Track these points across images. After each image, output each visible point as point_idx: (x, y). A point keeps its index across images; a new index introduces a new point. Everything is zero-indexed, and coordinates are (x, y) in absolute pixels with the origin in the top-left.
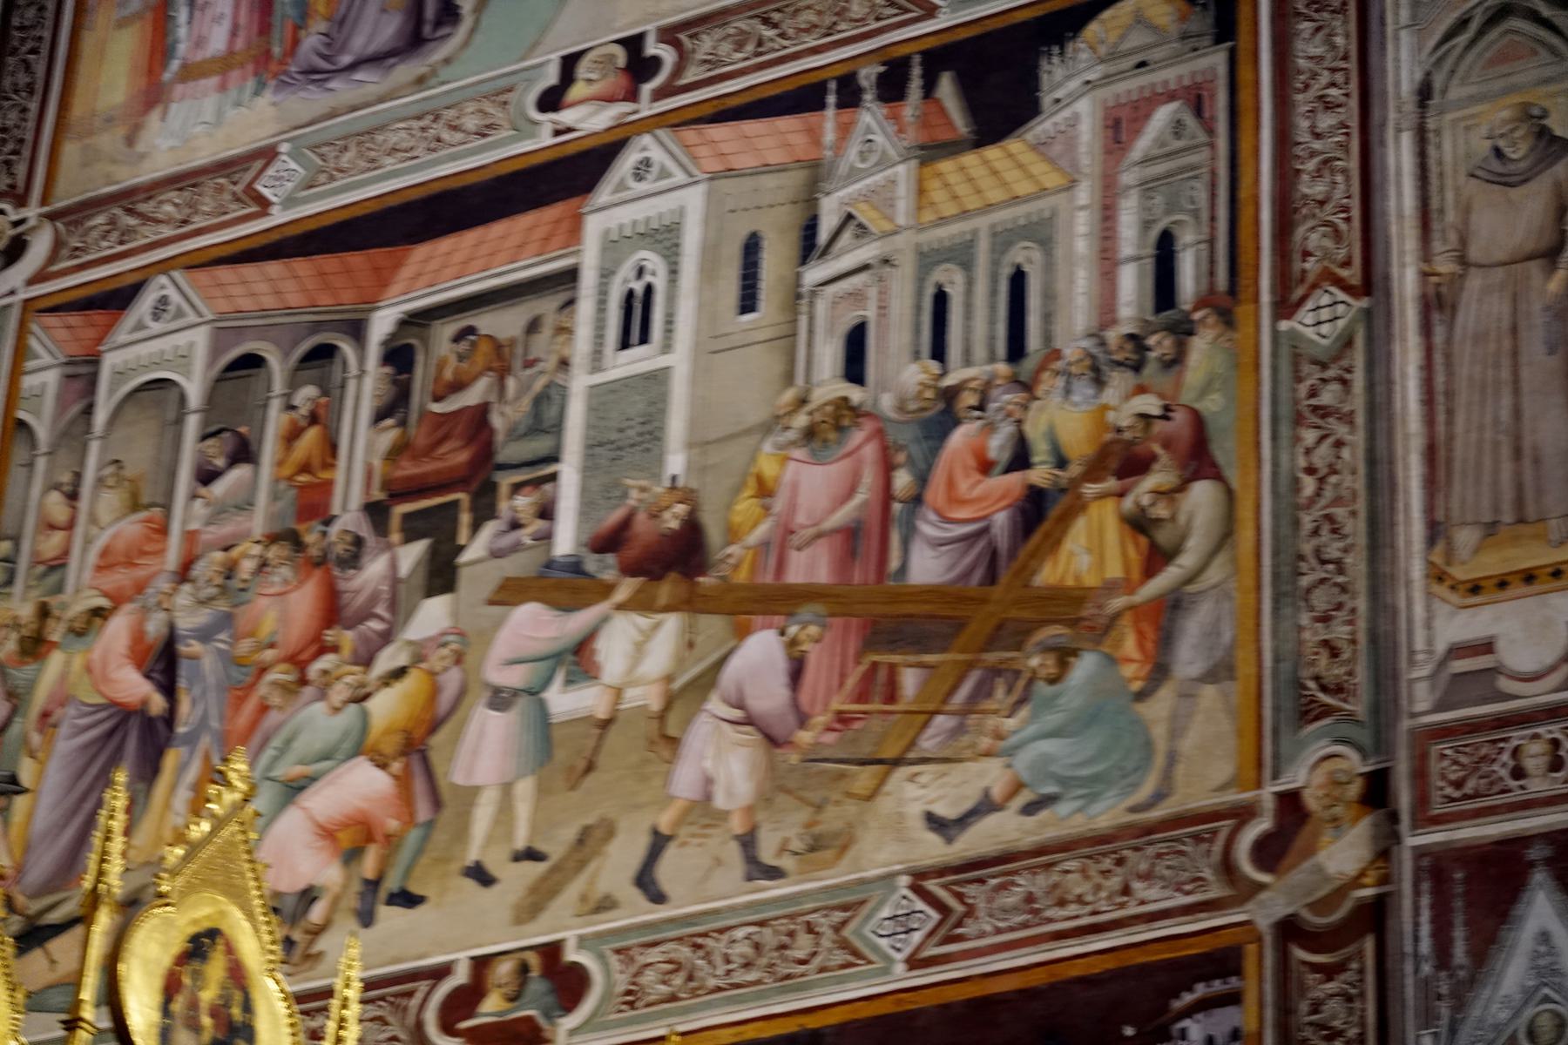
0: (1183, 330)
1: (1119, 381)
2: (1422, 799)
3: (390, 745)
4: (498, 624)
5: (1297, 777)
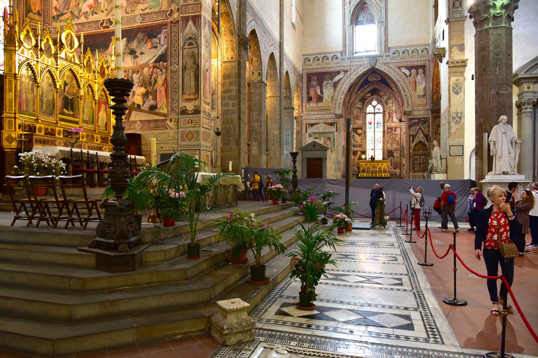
2: (181, 12)
5: (172, 8)
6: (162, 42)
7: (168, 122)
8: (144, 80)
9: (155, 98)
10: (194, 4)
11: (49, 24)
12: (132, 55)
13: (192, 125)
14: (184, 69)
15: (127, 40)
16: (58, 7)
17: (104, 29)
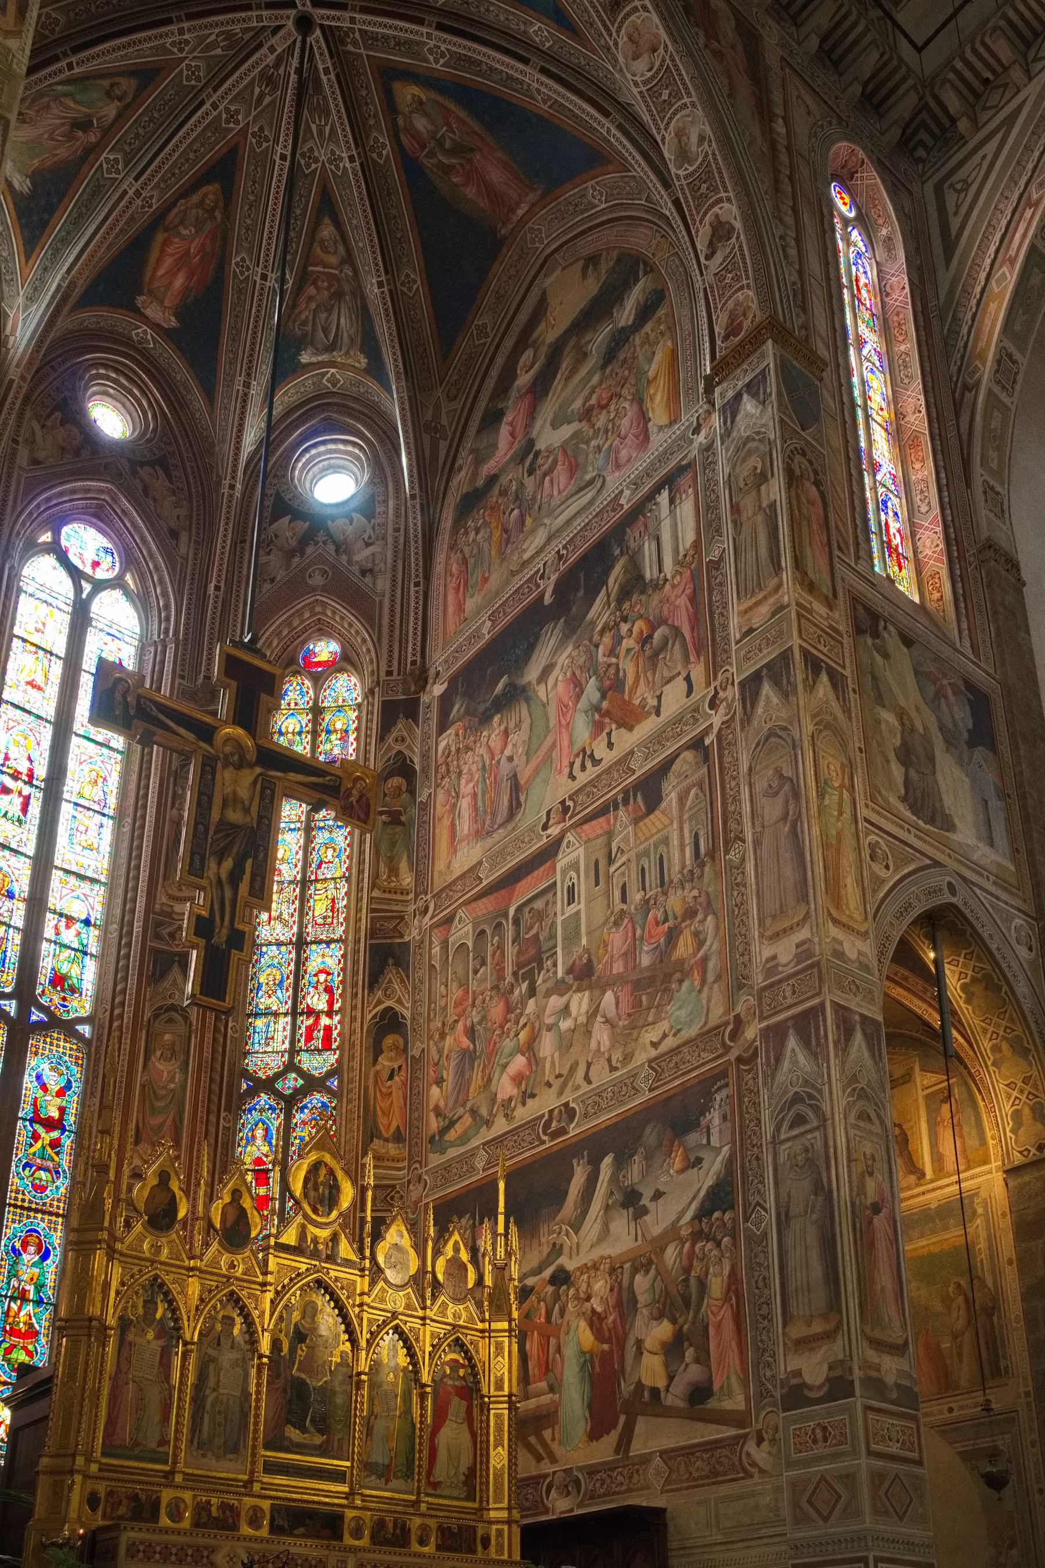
0: (702, 865)
1: (687, 886)
5: (738, 1009)
6: (715, 1141)
7: (751, 1447)
9: (703, 1358)
11: (420, 1163)
12: (631, 1210)
13: (827, 1451)
14: (784, 1219)
15: (615, 1159)
16: (442, 1104)
17: (552, 1140)
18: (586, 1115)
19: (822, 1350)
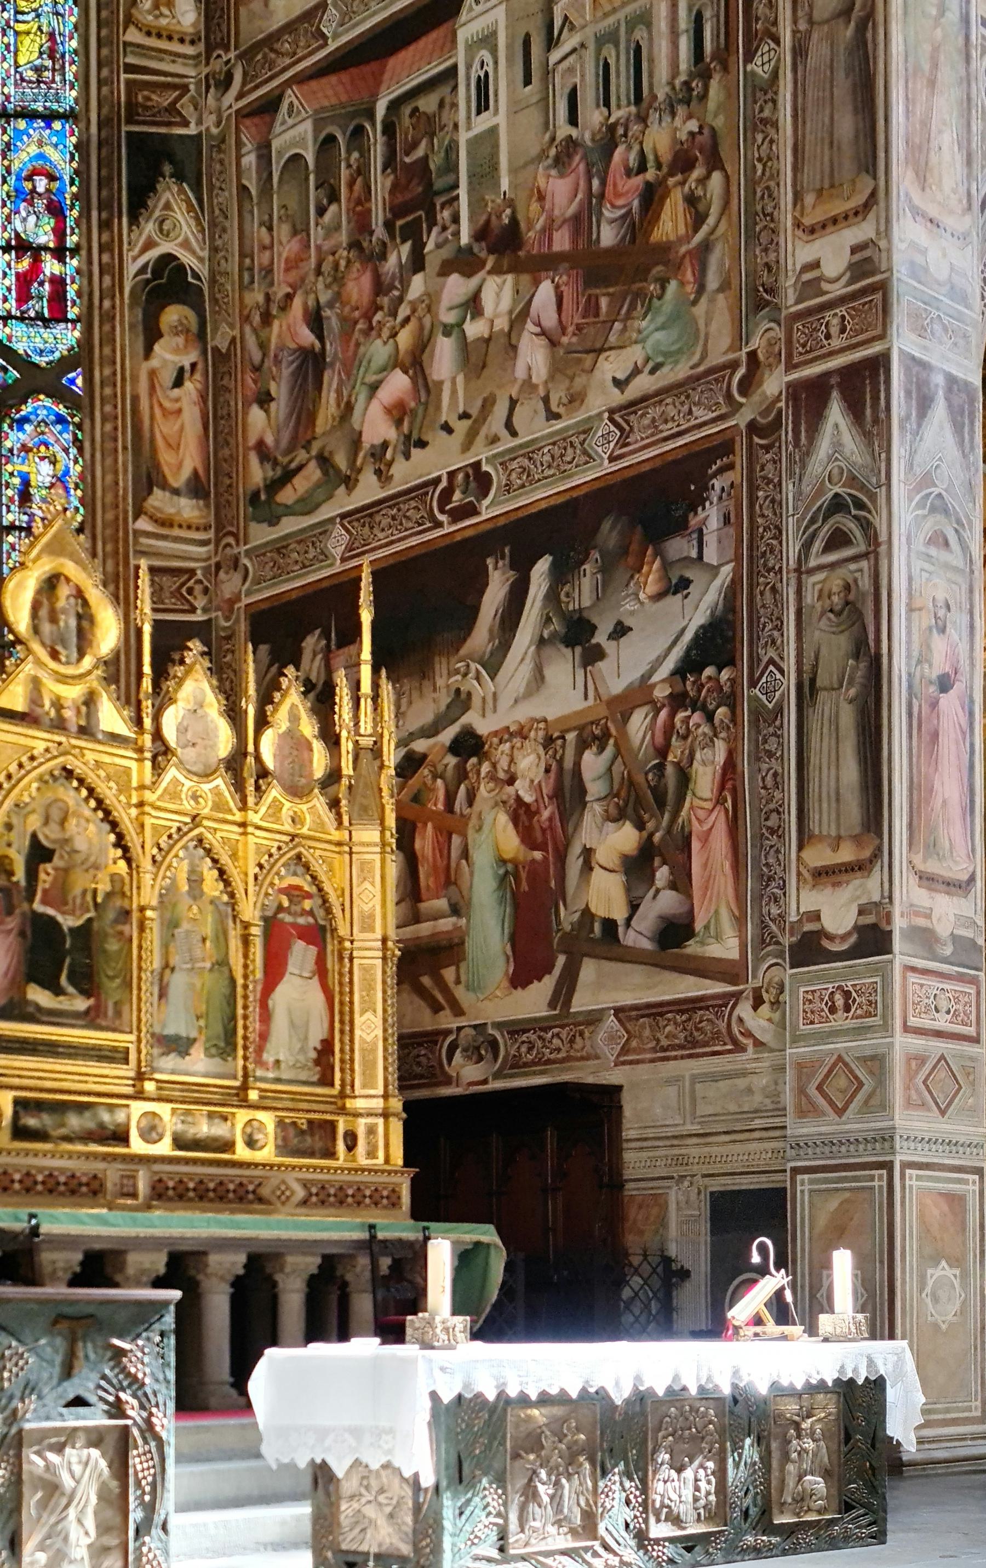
0: (706, 76)
1: (681, 110)
3: (408, 361)
4: (443, 286)
5: (756, 342)
7: (744, 1010)
8: (631, 783)
10: (853, 296)
11: (235, 536)
12: (578, 650)
15: (555, 567)
16: (269, 440)
17: (454, 520)
18: (508, 488)
19: (851, 887)
